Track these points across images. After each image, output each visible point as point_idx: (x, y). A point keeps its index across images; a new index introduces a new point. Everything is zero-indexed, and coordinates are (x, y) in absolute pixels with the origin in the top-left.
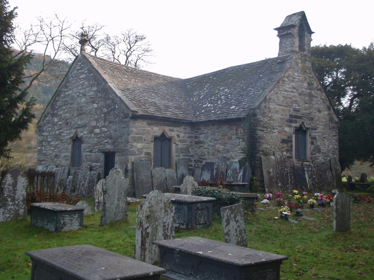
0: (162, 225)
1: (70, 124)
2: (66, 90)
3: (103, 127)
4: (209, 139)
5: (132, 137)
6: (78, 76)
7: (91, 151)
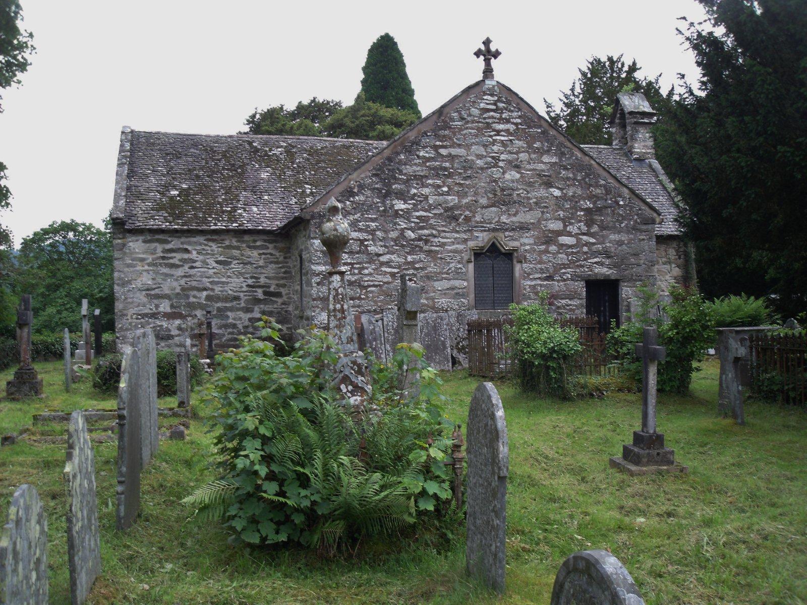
3: (584, 234)
7: (550, 278)
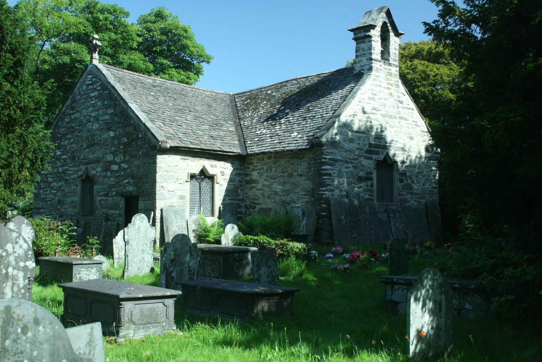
0: (188, 269)
1: (78, 158)
2: (71, 112)
3: (123, 162)
4: (264, 177)
6: (88, 94)
7: (107, 195)
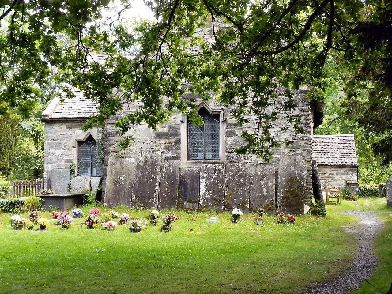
5: (48, 143)
